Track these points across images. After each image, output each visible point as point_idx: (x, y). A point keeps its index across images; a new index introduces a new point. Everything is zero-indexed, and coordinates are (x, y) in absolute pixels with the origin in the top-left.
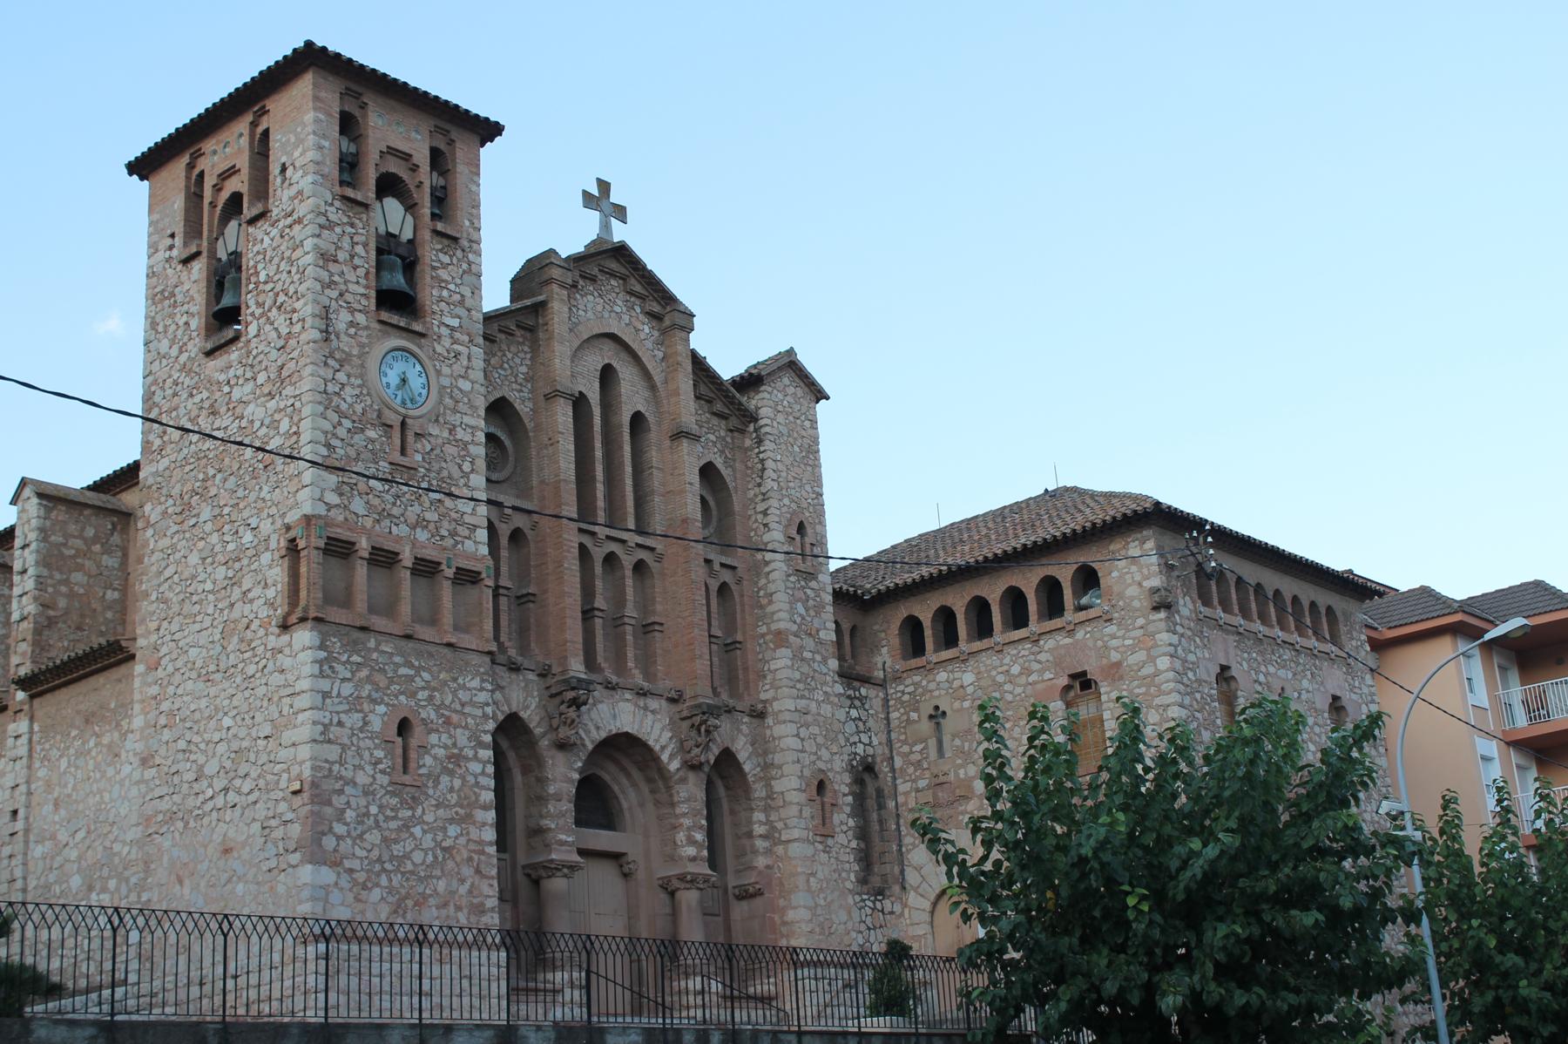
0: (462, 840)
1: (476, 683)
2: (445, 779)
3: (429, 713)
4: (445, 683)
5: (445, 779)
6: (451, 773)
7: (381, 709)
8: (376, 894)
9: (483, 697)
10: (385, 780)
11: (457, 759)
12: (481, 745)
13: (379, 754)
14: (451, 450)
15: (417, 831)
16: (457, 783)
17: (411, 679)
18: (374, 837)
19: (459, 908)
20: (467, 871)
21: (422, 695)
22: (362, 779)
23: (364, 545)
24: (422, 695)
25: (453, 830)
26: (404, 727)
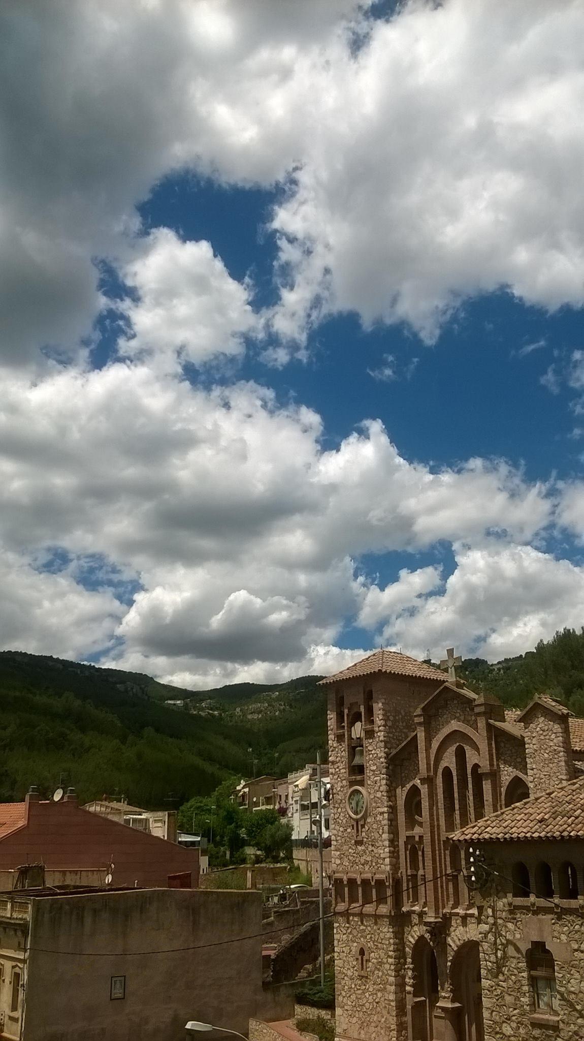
0: (383, 999)
1: (386, 930)
2: (376, 972)
3: (371, 944)
4: (375, 931)
5: (376, 972)
6: (379, 970)
7: (355, 944)
8: (354, 1020)
9: (388, 935)
10: (356, 974)
11: (381, 963)
12: (389, 956)
13: (355, 963)
14: (375, 826)
15: (367, 995)
16: (380, 974)
17: (364, 931)
18: (353, 997)
19: (382, 1028)
20: (385, 1012)
21: (368, 937)
22: (349, 973)
23: (345, 878)
24: (368, 937)
25: (379, 994)
26: (362, 952)
